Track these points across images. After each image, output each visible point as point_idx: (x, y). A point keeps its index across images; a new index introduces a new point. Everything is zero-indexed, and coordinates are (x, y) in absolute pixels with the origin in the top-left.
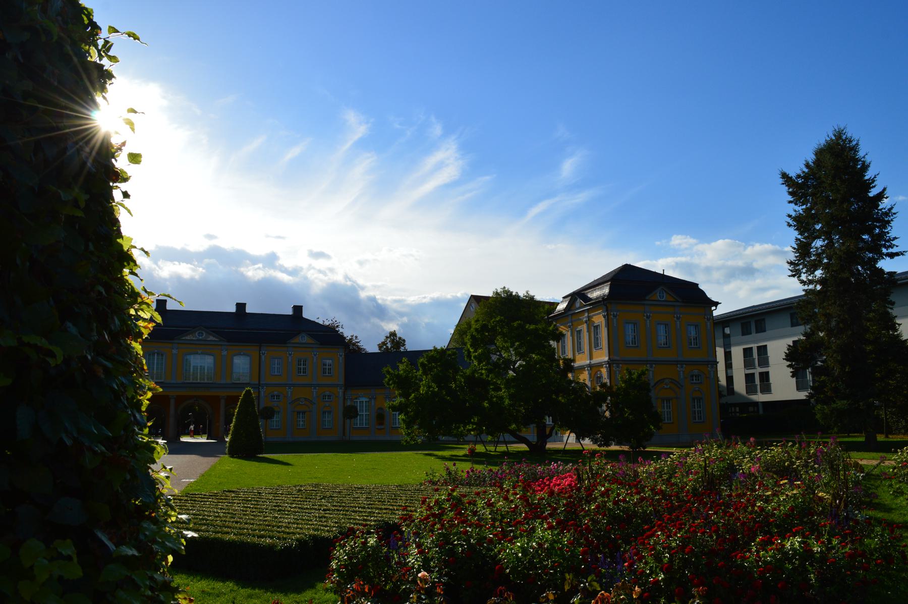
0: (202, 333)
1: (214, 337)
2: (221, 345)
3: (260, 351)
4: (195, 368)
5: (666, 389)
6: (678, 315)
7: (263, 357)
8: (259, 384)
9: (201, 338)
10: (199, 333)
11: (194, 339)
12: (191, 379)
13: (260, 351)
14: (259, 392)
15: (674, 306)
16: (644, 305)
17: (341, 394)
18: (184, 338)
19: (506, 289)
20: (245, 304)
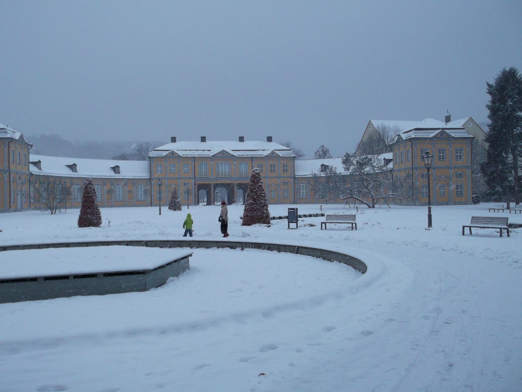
7: (254, 164)
12: (220, 176)
17: (293, 182)
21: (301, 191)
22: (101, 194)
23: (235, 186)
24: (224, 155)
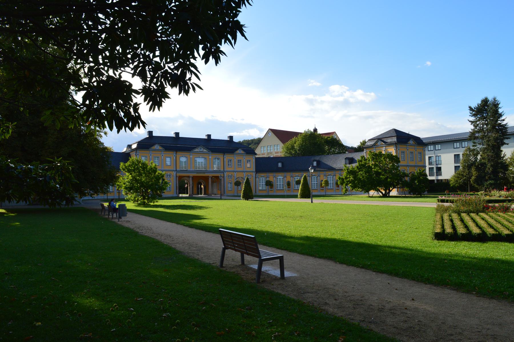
0: (201, 148)
3: (224, 156)
4: (199, 162)
8: (224, 171)
13: (224, 156)
14: (224, 174)
15: (415, 146)
16: (406, 145)
17: (254, 176)
18: (194, 151)
19: (309, 130)
21: (264, 184)
22: (283, 184)
23: (210, 179)
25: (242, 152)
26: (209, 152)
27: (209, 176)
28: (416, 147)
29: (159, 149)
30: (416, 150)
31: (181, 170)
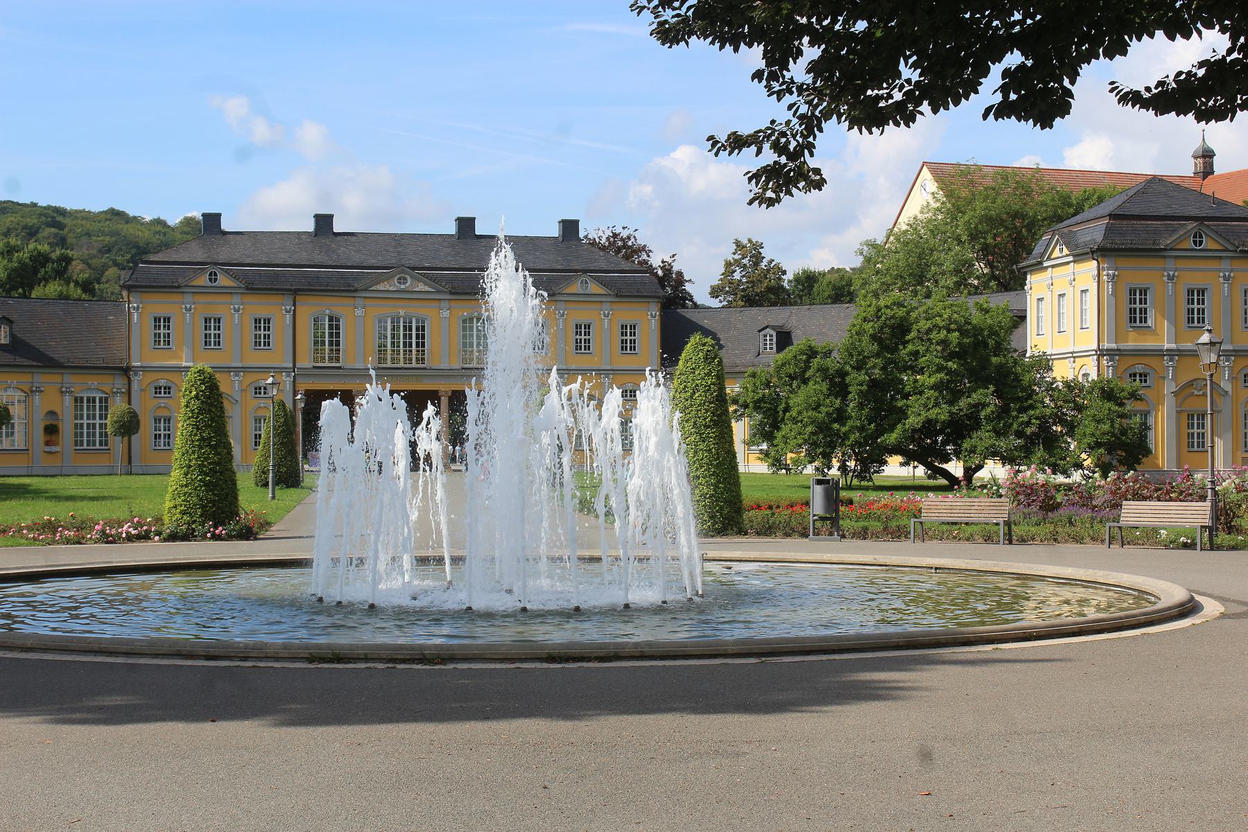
0: (405, 279)
1: (426, 284)
2: (440, 300)
5: (1196, 395)
6: (1227, 274)
9: (403, 286)
10: (400, 279)
11: (391, 289)
15: (1220, 258)
16: (1164, 257)
20: (473, 220)
24: (403, 286)
25: (594, 288)
26: (438, 292)
27: (351, 391)
28: (1225, 264)
29: (223, 284)
30: (1226, 279)
31: (315, 367)
